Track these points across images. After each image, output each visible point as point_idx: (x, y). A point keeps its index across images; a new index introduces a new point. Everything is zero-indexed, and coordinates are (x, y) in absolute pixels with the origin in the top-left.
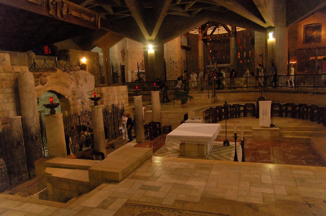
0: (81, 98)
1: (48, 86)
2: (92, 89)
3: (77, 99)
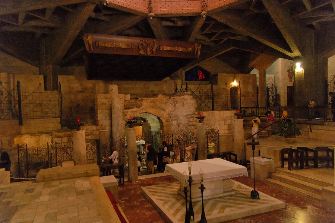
0: (176, 120)
1: (143, 109)
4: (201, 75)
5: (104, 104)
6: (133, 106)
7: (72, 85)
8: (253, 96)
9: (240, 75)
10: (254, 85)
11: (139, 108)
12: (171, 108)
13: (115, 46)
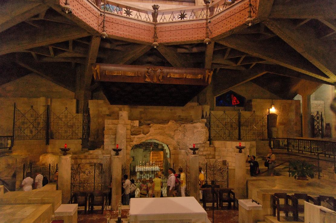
0: (185, 149)
1: (150, 136)
2: (201, 142)
3: (180, 149)
4: (234, 100)
5: (111, 129)
6: (140, 133)
7: (100, 109)
8: (296, 124)
9: (279, 102)
10: (297, 113)
11: (146, 134)
12: (180, 135)
13: (122, 75)
